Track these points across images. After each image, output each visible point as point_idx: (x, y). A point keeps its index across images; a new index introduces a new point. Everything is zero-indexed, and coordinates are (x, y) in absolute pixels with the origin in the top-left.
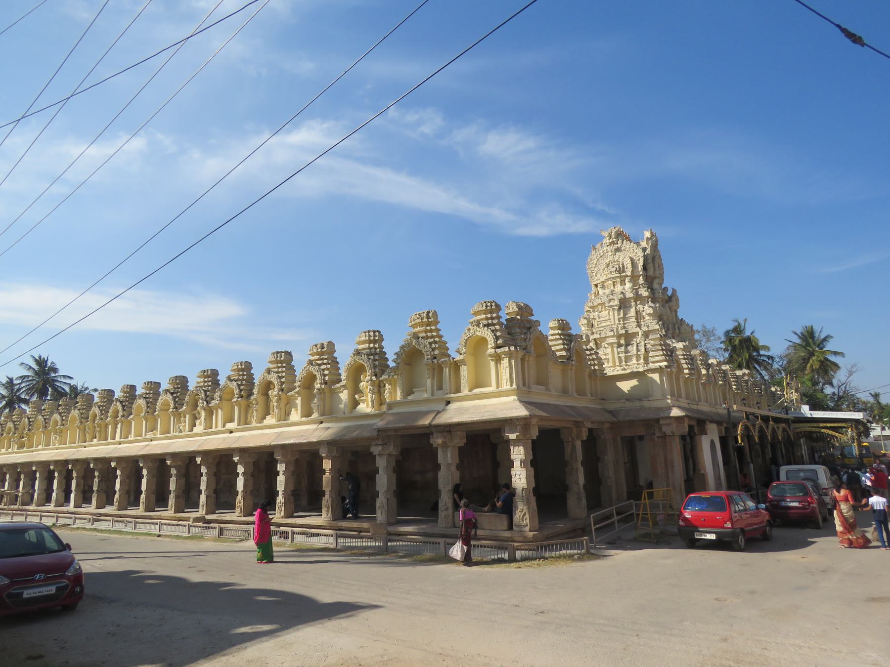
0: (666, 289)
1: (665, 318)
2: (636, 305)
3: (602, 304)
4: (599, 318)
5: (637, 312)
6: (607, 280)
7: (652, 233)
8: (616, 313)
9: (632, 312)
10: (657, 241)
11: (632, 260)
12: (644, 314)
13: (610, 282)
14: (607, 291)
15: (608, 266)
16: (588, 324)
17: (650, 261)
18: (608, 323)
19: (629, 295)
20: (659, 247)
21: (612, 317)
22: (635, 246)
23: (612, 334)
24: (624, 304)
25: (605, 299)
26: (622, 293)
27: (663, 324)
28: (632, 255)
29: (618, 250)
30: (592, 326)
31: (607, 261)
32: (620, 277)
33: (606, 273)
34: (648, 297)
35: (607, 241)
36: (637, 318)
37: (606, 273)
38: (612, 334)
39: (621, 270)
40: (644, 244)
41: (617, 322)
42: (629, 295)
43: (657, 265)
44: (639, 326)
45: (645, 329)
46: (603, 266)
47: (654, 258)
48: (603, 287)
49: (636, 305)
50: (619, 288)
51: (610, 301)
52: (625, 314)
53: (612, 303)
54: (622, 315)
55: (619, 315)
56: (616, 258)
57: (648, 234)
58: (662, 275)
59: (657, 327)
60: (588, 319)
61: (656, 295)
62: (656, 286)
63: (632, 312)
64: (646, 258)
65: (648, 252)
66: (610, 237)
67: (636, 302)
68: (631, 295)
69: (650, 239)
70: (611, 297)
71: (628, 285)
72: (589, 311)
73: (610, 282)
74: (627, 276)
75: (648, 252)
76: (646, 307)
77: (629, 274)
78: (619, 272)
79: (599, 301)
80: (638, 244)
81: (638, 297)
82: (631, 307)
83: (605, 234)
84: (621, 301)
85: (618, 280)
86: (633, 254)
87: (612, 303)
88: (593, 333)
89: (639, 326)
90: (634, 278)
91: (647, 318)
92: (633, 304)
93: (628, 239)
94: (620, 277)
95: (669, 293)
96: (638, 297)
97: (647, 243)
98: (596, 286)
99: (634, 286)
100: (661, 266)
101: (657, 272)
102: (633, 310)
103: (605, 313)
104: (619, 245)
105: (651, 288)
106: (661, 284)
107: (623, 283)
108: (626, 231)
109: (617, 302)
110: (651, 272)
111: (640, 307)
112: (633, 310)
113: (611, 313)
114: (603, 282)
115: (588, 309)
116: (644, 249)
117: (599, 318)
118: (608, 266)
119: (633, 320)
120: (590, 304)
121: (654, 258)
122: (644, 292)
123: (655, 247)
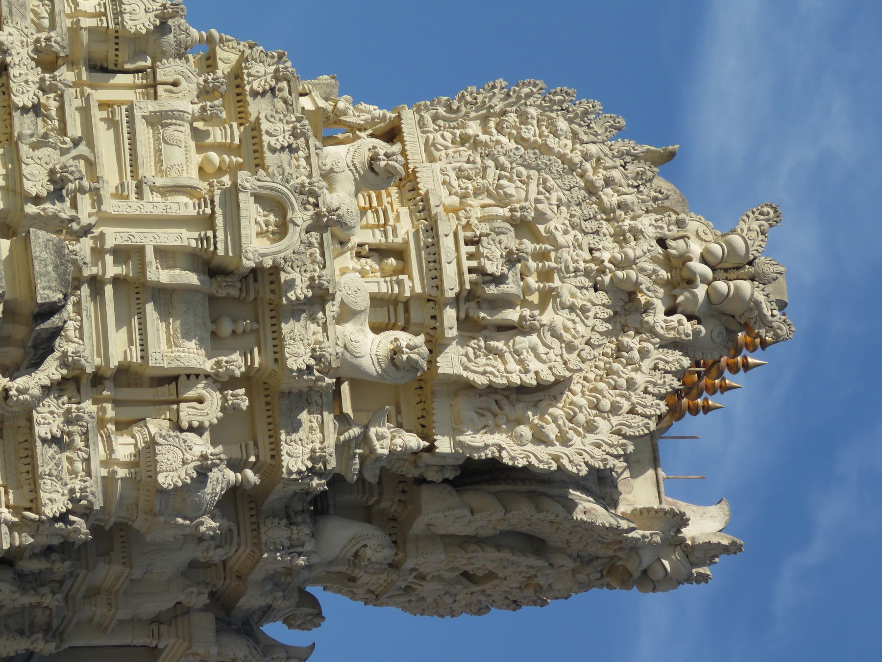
0: (309, 613)
1: (107, 573)
2: (223, 382)
3: (252, 149)
4: (158, 121)
5: (172, 383)
6: (422, 208)
7: (708, 552)
8: (187, 238)
9: (172, 347)
10: (647, 580)
11: (543, 393)
12: (157, 426)
13: (404, 227)
14: (342, 197)
15: (523, 226)
16: (118, 37)
17: (523, 516)
18: (110, 173)
19: (300, 343)
20: (599, 596)
21: (154, 204)
22: (638, 426)
23: (36, 181)
24: (236, 297)
25: (284, 171)
26: (320, 296)
27: (65, 548)
28: (578, 395)
29: (626, 307)
30: (101, 68)
31: (557, 223)
32: (433, 300)
33: (476, 208)
34: (270, 466)
35: (698, 241)
36: (125, 375)
37: (476, 208)
38: (36, 181)
39: (481, 310)
40: (640, 493)
41: (114, 237)
42: (300, 343)
43: (484, 560)
44: (74, 383)
45: (48, 420)
46: (523, 193)
47: (535, 545)
48: (373, 176)
49: (223, 382)
50: (355, 280)
51: (273, 203)
52: (166, 298)
53: (252, 215)
54: (160, 274)
55: (165, 254)
56: (567, 289)
57: (705, 524)
58: (408, 595)
59: (53, 501)
60: (151, 44)
61: (276, 532)
62: (341, 535)
63: (172, 347)
64: (544, 486)
65: (587, 509)
66: (728, 266)
67: (247, 380)
68: (297, 356)
69: (674, 542)
70: (301, 217)
71: (370, 347)
72: (209, 63)
73: (404, 227)
74: (436, 345)
75: (587, 509)
76: (200, 445)
77: (452, 362)
78: (469, 298)
79: (276, 131)
80: (646, 452)
81: (277, 399)
82: (214, 343)
83: (746, 236)
84: (266, 277)
85: (413, 284)
86: (583, 398)
87: (252, 215)
88: (47, 61)
89: (74, 383)
90: (411, 389)
91: (124, 447)
92: (236, 363)
93: (683, 400)
94: (433, 300)
95: (275, 630)
96: (277, 399)
97: (643, 515)
98: (392, 134)
99: (362, 384)
100: (471, 591)
101: (434, 560)
102: (192, 355)
103: (184, 161)
104: (657, 318)
105: (326, 499)
106: (345, 580)
107: (389, 312)
108: (741, 396)
109: (257, 248)
110: (441, 513)
111: (208, 406)
112: (192, 355)
113: (185, 206)
114: (408, 183)
115: (227, 58)
116: (601, 483)
117: (158, 121)
118: (523, 226)
119: (120, 349)
120: (261, 73)
121: (535, 545)
122: (306, 446)
123: (617, 563)
